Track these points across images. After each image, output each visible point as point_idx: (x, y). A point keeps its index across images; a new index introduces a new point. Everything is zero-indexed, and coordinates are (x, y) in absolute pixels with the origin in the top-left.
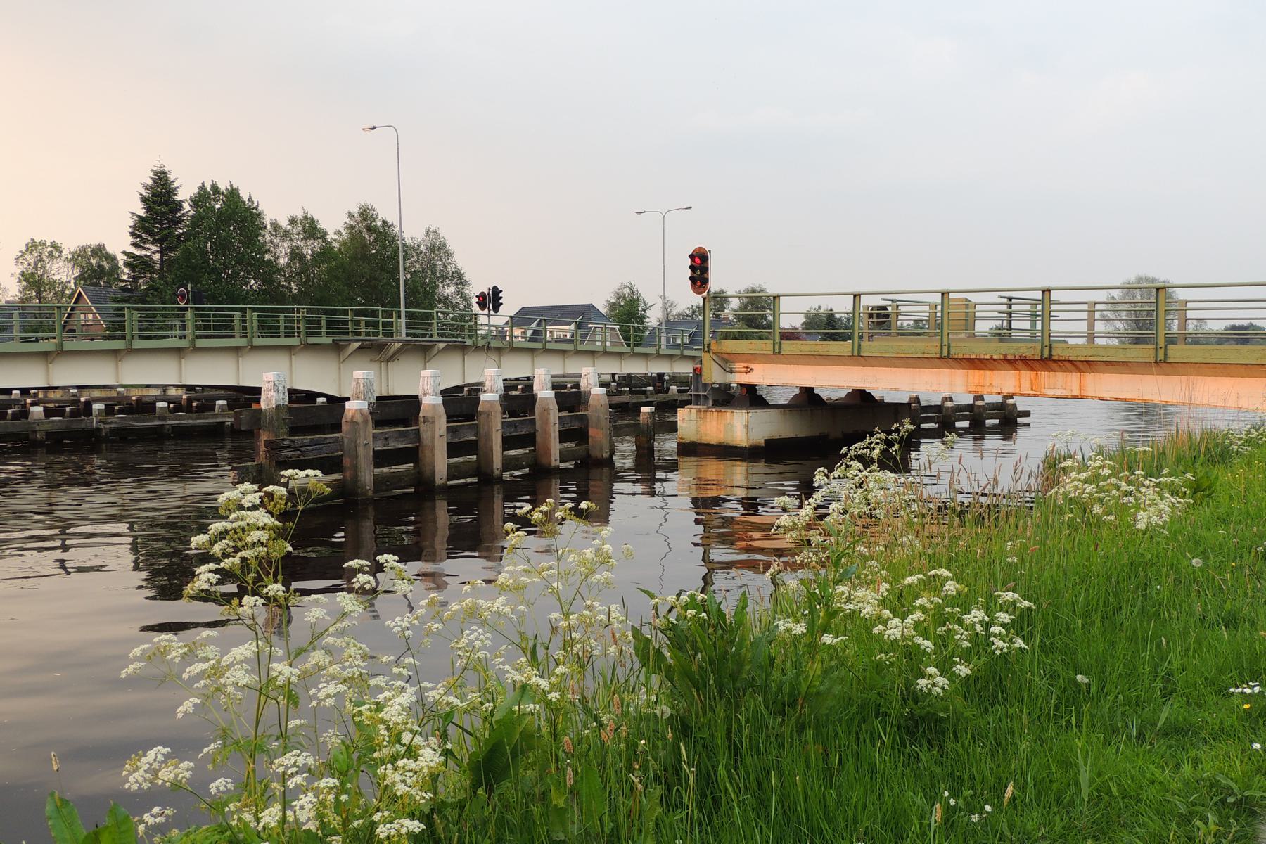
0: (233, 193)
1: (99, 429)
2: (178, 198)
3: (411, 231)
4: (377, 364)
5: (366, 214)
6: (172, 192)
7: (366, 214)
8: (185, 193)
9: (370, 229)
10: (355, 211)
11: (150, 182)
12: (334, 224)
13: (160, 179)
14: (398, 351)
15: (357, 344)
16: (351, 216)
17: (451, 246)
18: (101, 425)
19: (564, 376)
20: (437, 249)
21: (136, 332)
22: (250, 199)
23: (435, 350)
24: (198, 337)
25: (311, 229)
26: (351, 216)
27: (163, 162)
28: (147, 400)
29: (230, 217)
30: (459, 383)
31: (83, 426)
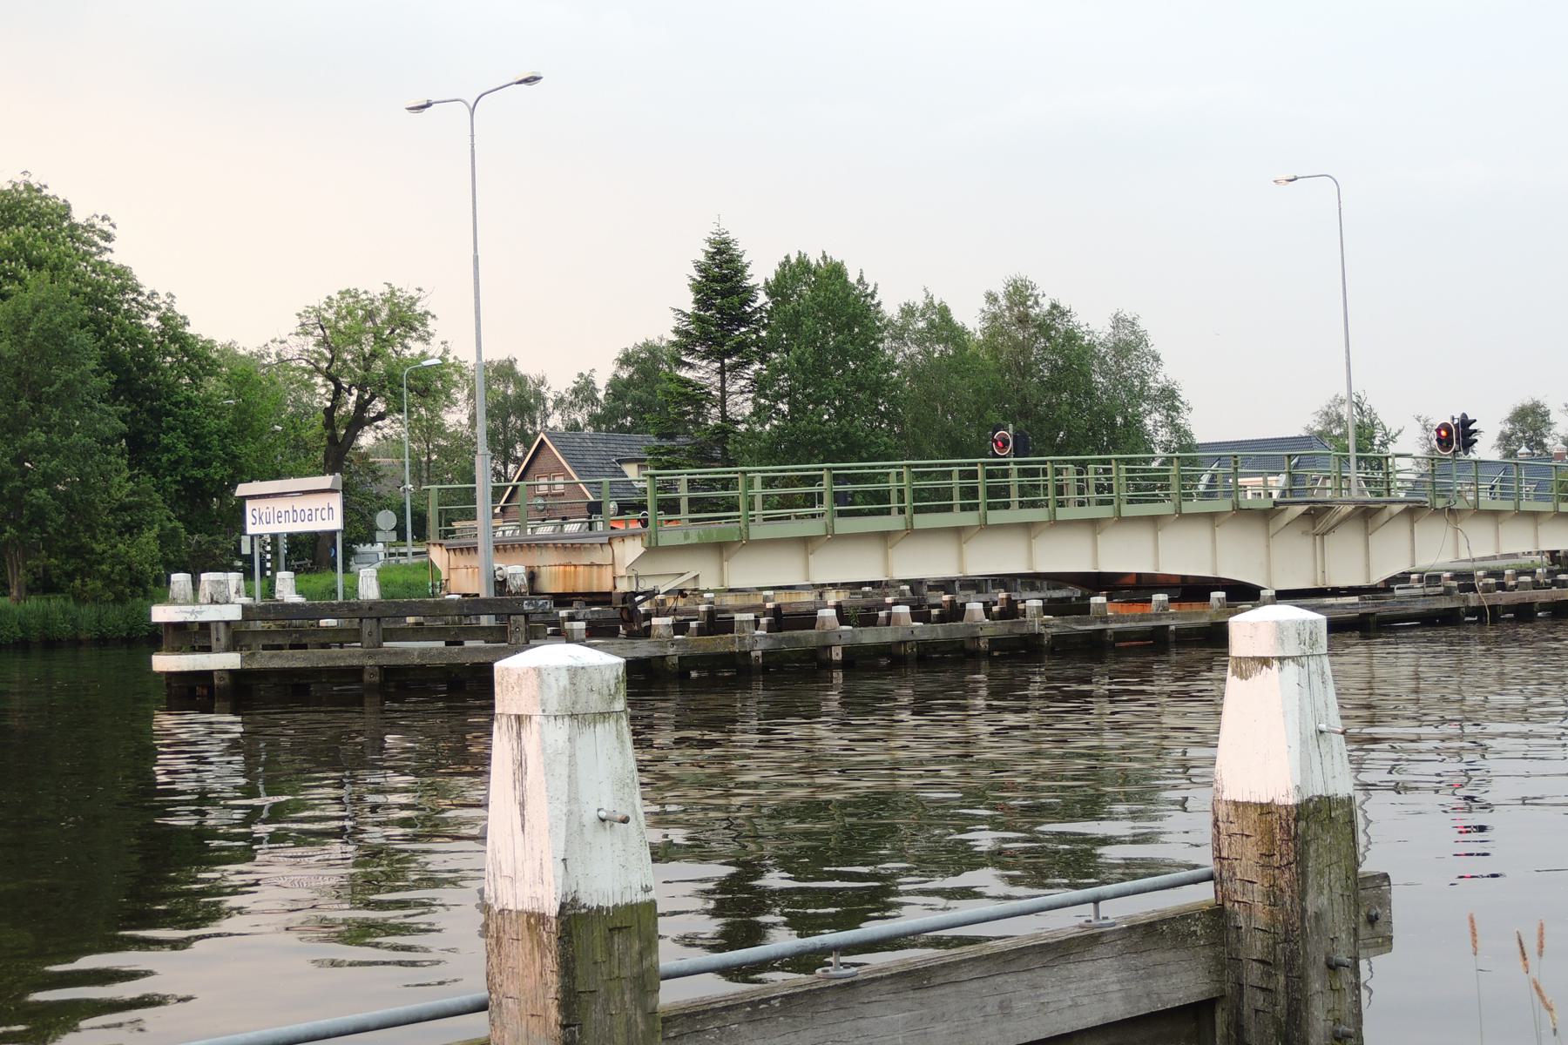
0: (837, 271)
1: (1040, 635)
2: (750, 282)
3: (1093, 321)
4: (1310, 540)
5: (1019, 293)
6: (739, 271)
7: (1019, 293)
8: (760, 271)
9: (1023, 320)
10: (999, 289)
11: (702, 258)
12: (970, 317)
13: (720, 252)
14: (1347, 518)
15: (1301, 509)
16: (992, 298)
17: (1156, 343)
18: (1043, 630)
19: (1494, 558)
20: (1129, 345)
21: (758, 511)
22: (861, 280)
23: (1385, 515)
24: (917, 510)
25: (942, 325)
26: (992, 298)
27: (725, 226)
28: (803, 609)
29: (824, 307)
30: (1405, 568)
31: (1025, 631)
